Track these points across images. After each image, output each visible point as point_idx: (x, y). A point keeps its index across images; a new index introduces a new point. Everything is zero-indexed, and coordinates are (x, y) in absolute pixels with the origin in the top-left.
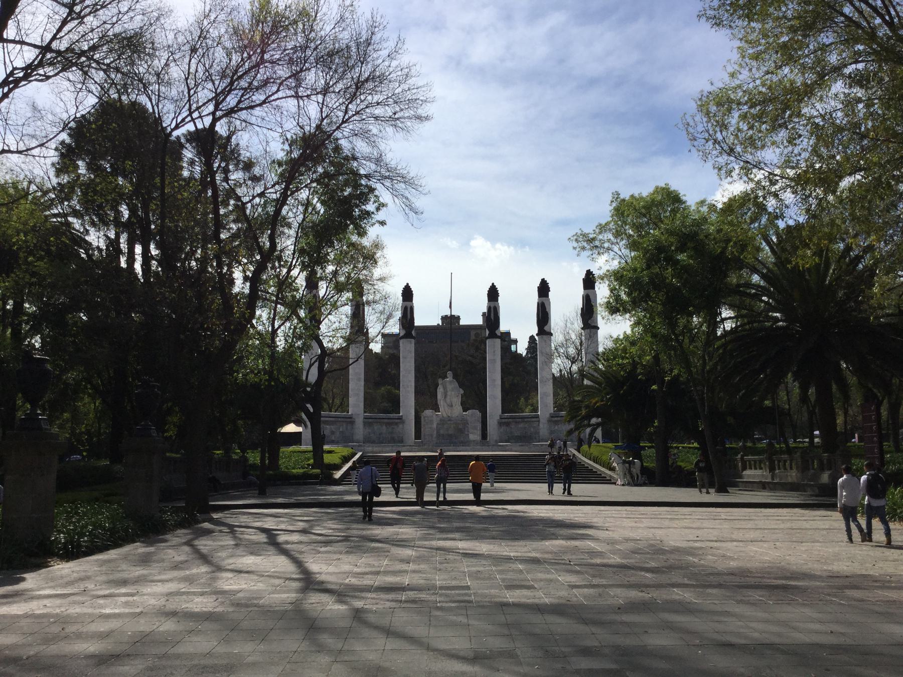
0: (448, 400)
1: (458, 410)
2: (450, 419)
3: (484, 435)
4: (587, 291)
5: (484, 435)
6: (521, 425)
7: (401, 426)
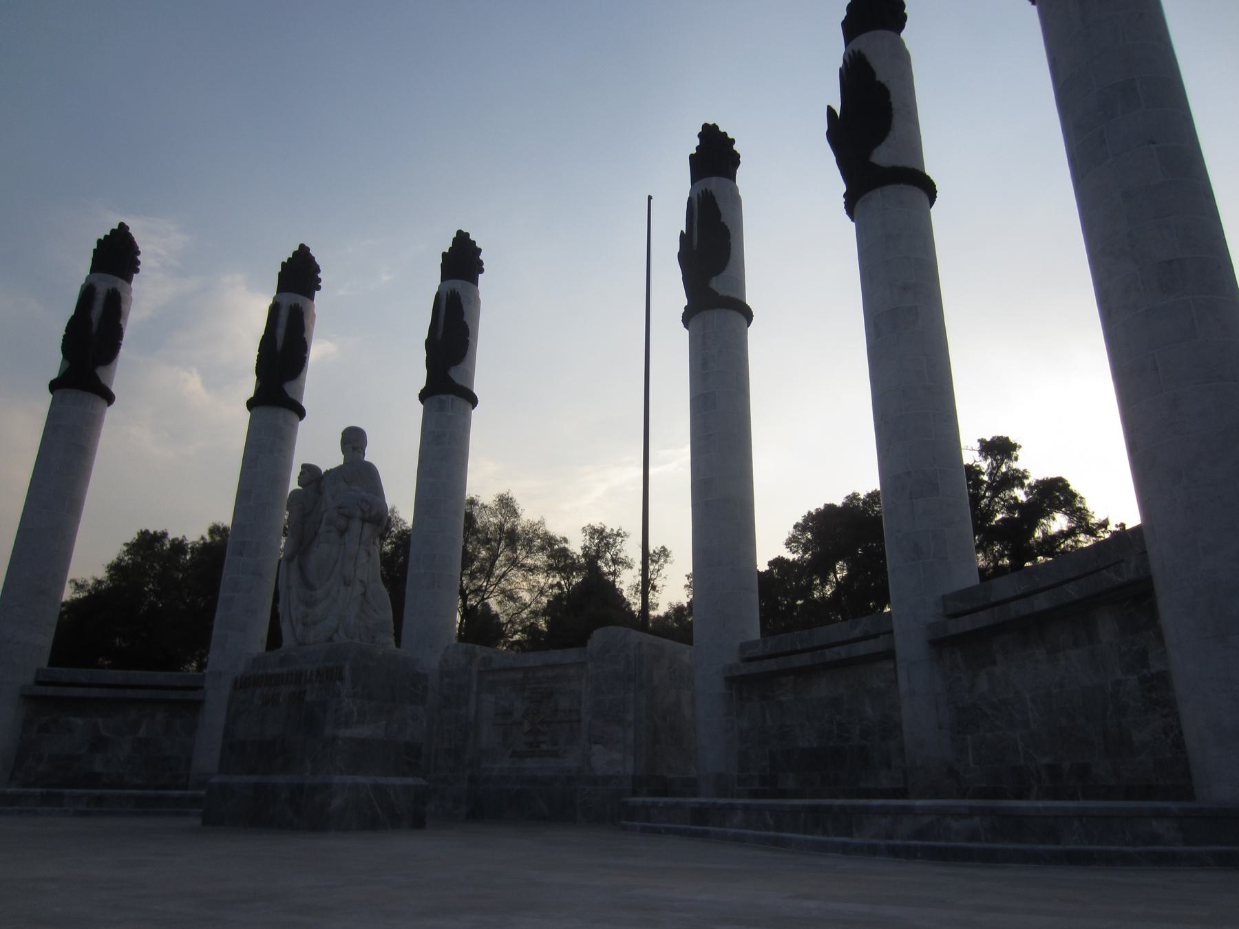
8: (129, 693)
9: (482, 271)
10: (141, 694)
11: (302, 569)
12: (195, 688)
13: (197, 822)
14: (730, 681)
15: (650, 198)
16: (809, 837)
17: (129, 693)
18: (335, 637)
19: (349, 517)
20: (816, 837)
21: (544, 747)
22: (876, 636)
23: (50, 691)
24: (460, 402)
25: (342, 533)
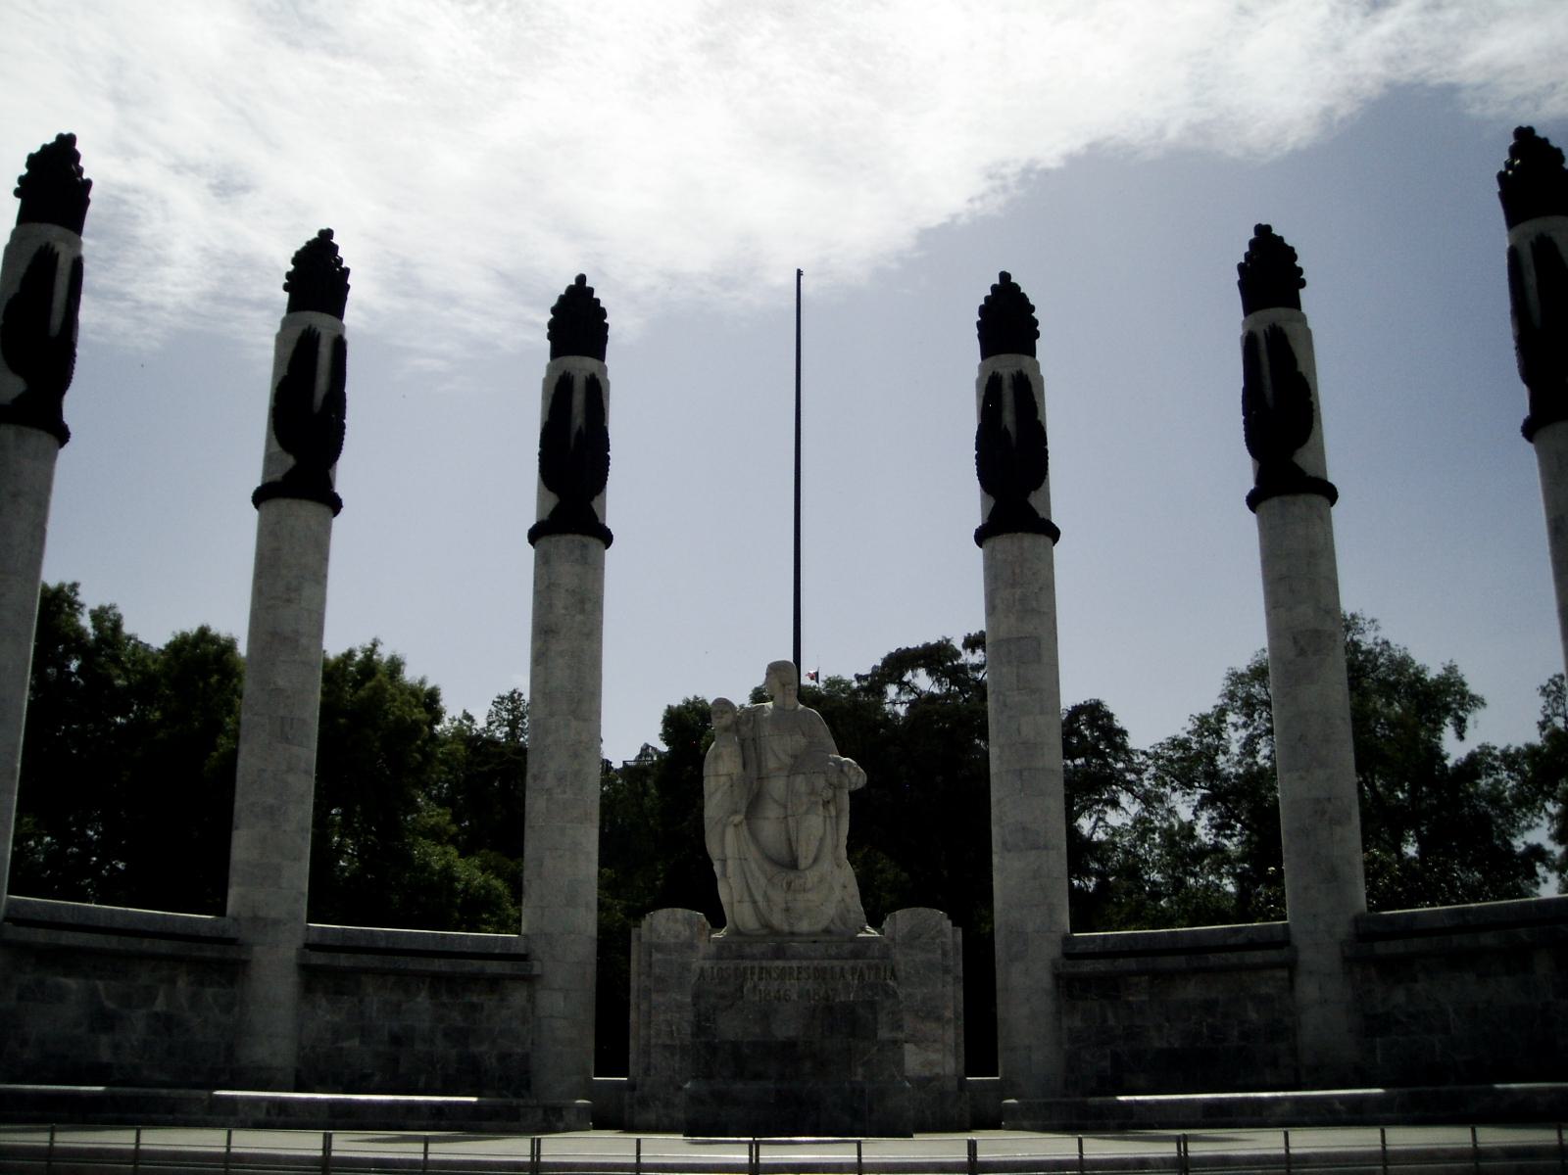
0: (770, 828)
1: (831, 889)
2: (778, 942)
3: (981, 1041)
4: (1532, 227)
5: (981, 1041)
6: (1191, 991)
7: (518, 997)
8: (146, 945)
10: (164, 946)
14: (1057, 977)
17: (146, 945)
18: (832, 927)
19: (836, 788)
23: (41, 936)
25: (826, 804)
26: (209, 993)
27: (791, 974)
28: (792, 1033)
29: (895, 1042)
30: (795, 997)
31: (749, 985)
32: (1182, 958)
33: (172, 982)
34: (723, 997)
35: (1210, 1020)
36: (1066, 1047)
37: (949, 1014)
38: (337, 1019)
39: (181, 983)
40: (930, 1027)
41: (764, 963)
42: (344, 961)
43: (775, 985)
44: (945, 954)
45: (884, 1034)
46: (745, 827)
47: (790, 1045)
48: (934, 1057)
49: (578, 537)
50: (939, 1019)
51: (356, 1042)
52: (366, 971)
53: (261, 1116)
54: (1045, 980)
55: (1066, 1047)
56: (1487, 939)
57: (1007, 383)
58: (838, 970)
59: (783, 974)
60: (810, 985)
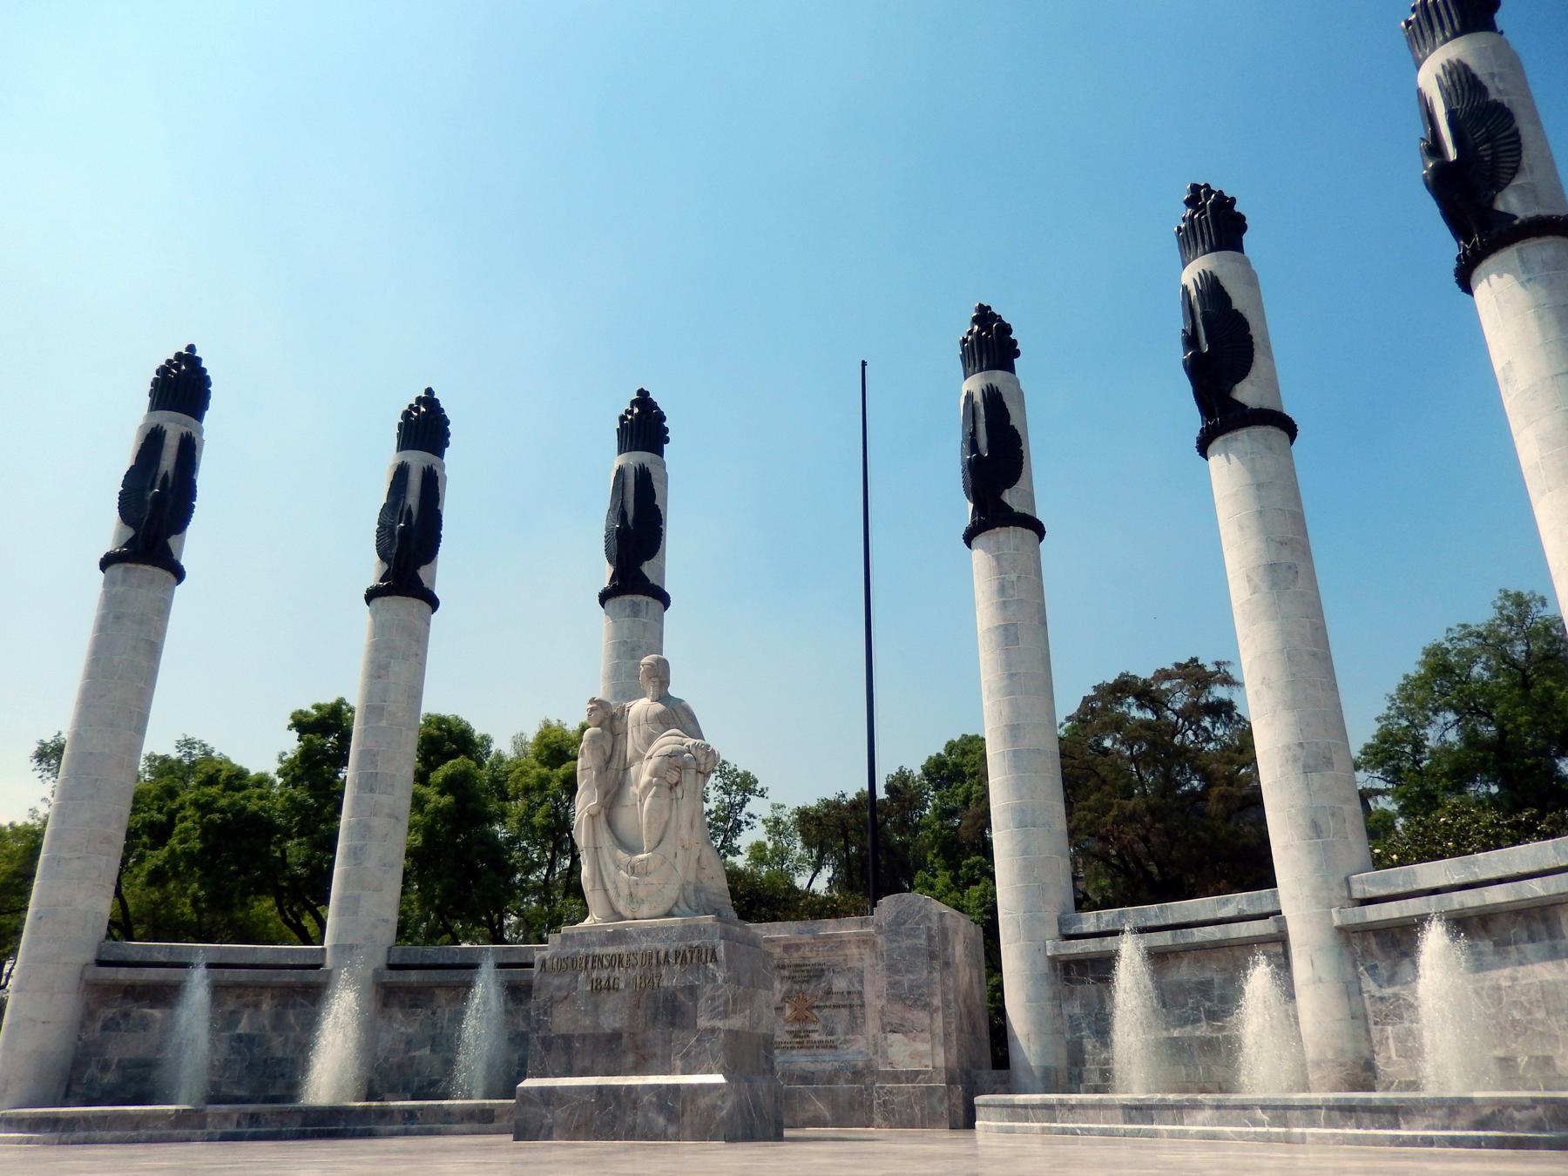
9: (667, 441)
10: (243, 975)
11: (611, 824)
12: (317, 967)
13: (511, 1137)
15: (864, 364)
16: (1339, 1131)
18: (676, 910)
20: (1348, 1131)
21: (815, 1037)
22: (1265, 916)
24: (656, 604)
26: (291, 1016)
27: (620, 962)
28: (617, 1025)
29: (713, 1031)
30: (622, 986)
31: (582, 976)
32: (1168, 934)
33: (257, 1005)
34: (559, 988)
35: (1208, 1004)
36: (1068, 1036)
37: (937, 1001)
38: (410, 1030)
39: (267, 1006)
40: (920, 1017)
41: (598, 951)
42: (414, 976)
43: (604, 974)
44: (930, 938)
45: (703, 1022)
46: (602, 818)
47: (616, 1036)
48: (926, 1047)
49: (628, 598)
50: (926, 1006)
51: (427, 1051)
52: (439, 986)
53: (231, 1128)
54: (1043, 966)
55: (1068, 1036)
56: (1496, 896)
57: (978, 398)
58: (662, 954)
59: (617, 961)
60: (636, 973)
